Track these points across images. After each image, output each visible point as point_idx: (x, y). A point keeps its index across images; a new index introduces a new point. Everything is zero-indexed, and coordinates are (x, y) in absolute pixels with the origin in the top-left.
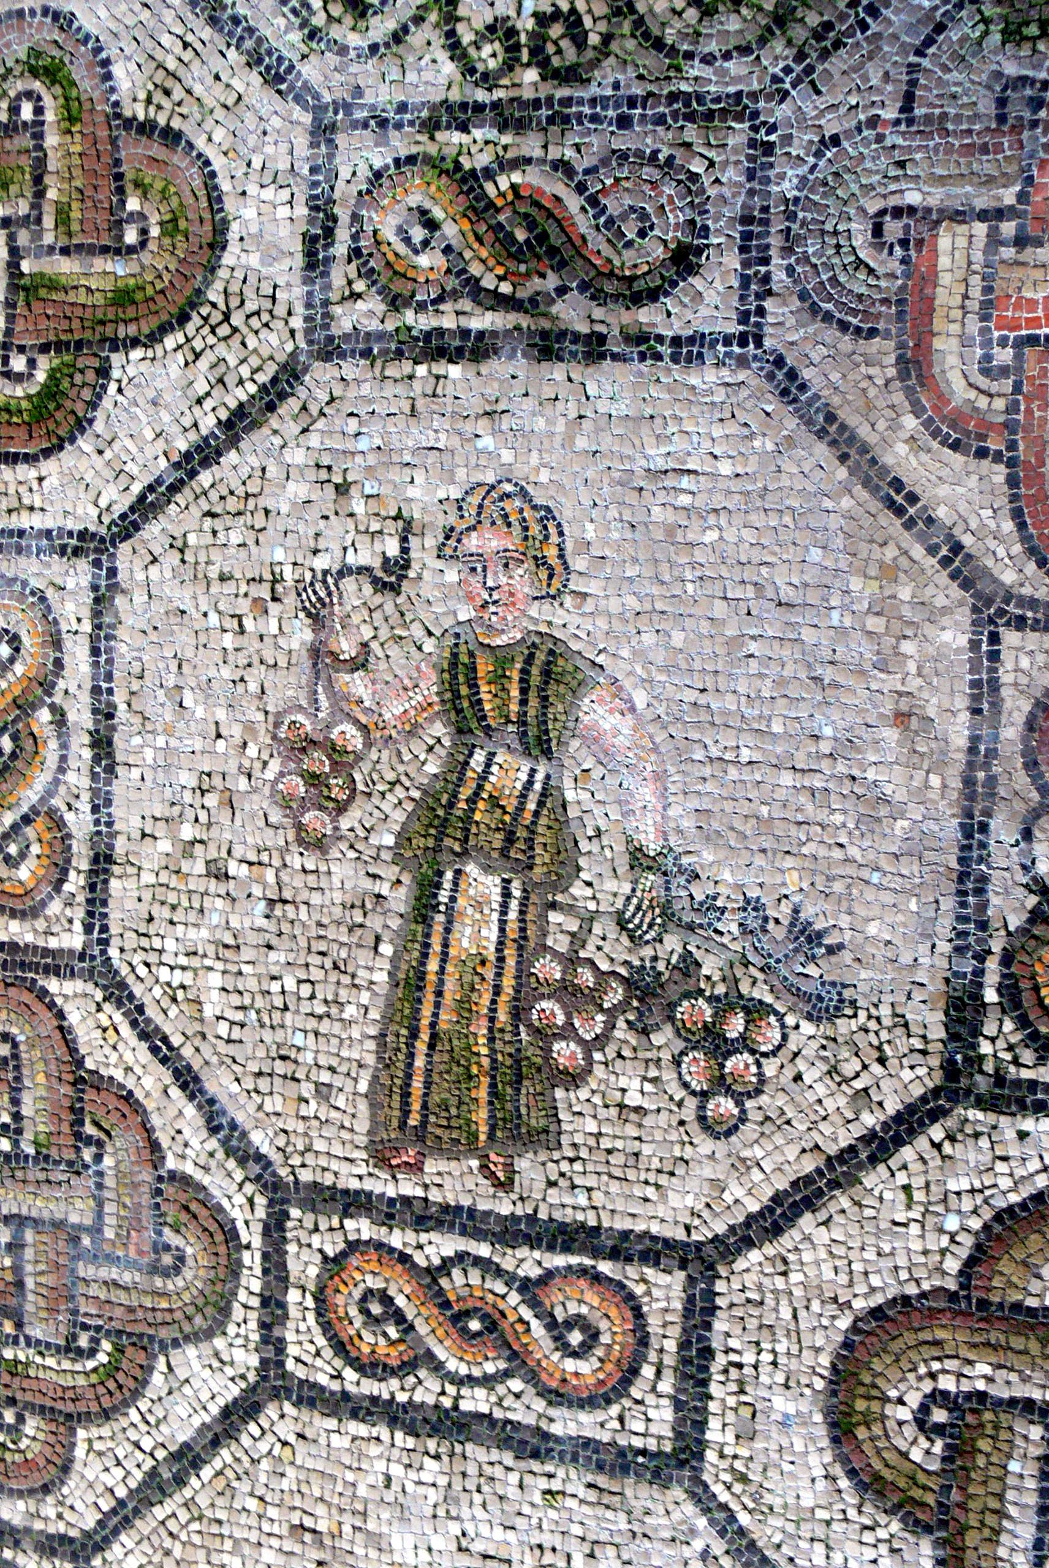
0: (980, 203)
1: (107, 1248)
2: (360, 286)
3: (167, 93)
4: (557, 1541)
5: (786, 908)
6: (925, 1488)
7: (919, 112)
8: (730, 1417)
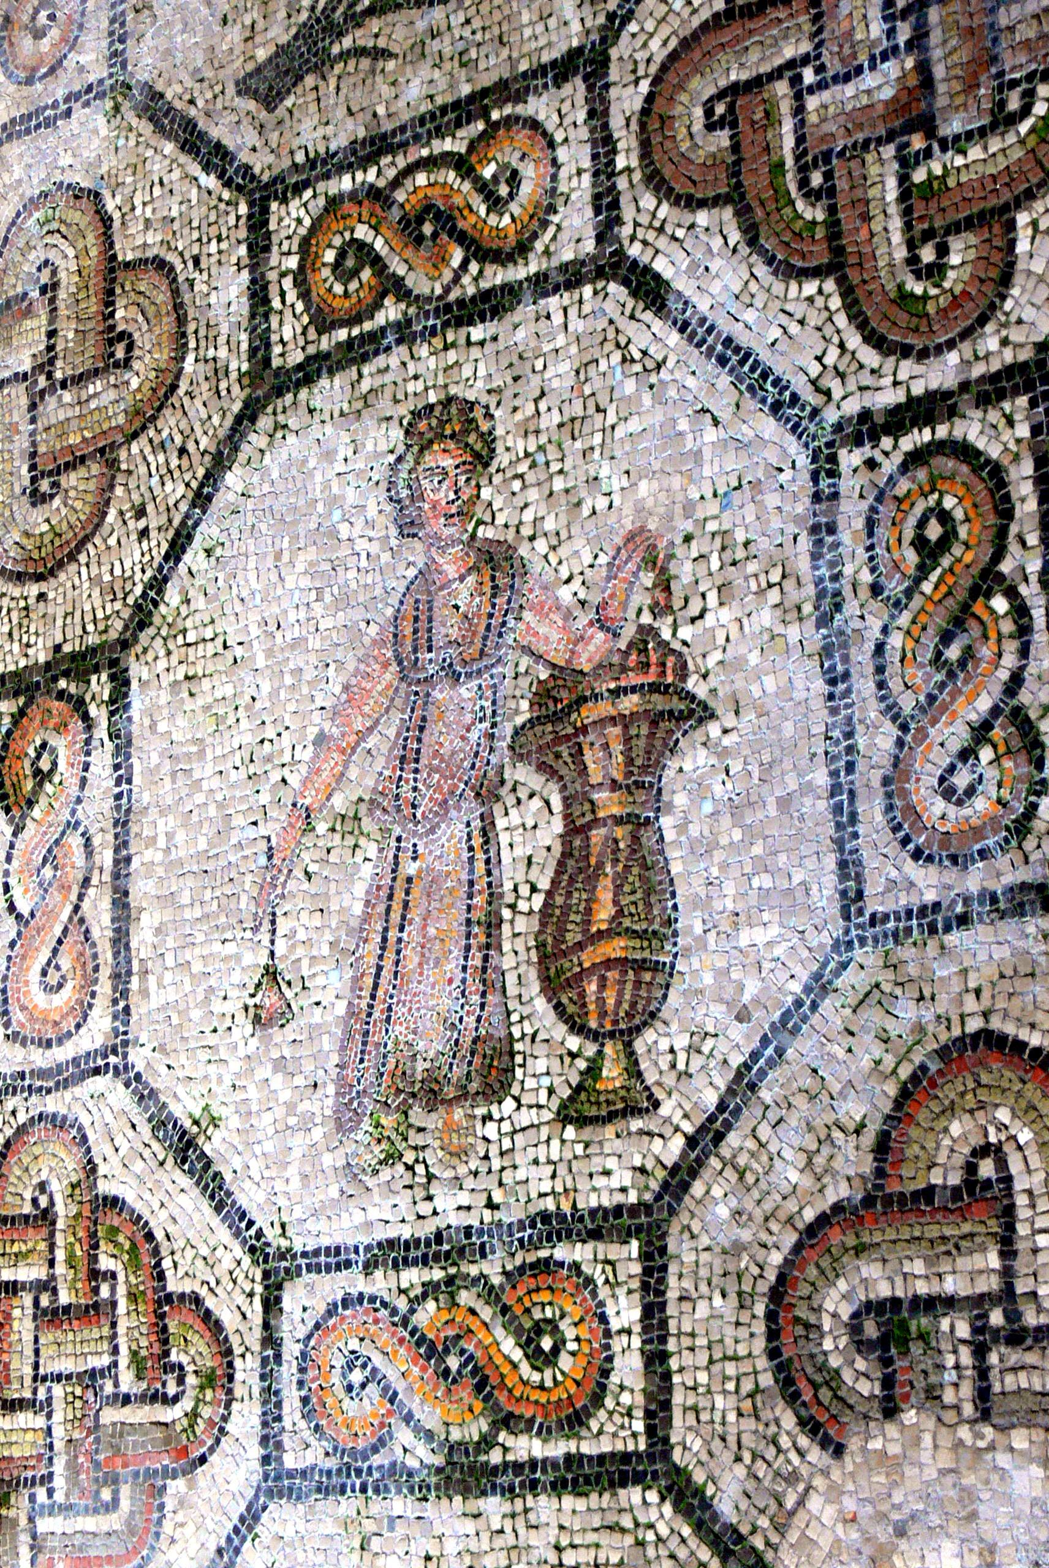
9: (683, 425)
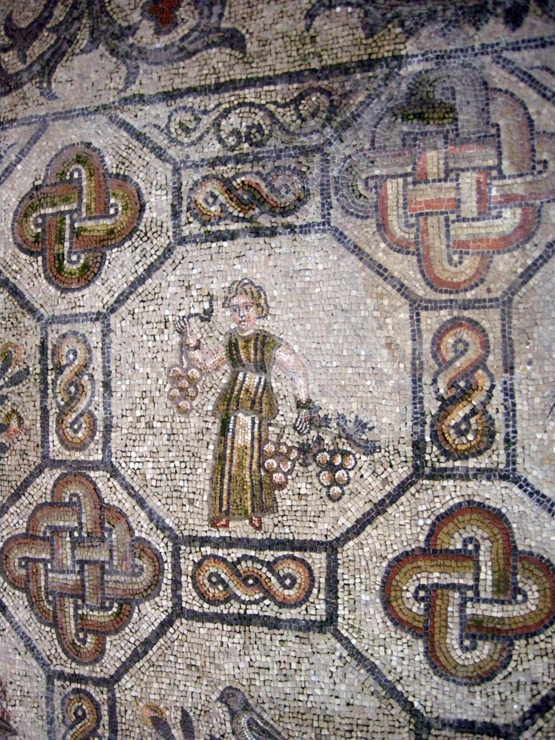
0: (400, 172)
1: (114, 568)
2: (191, 219)
3: (123, 164)
4: (286, 658)
5: (353, 416)
6: (419, 621)
7: (377, 145)
8: (346, 604)
9: (10, 650)
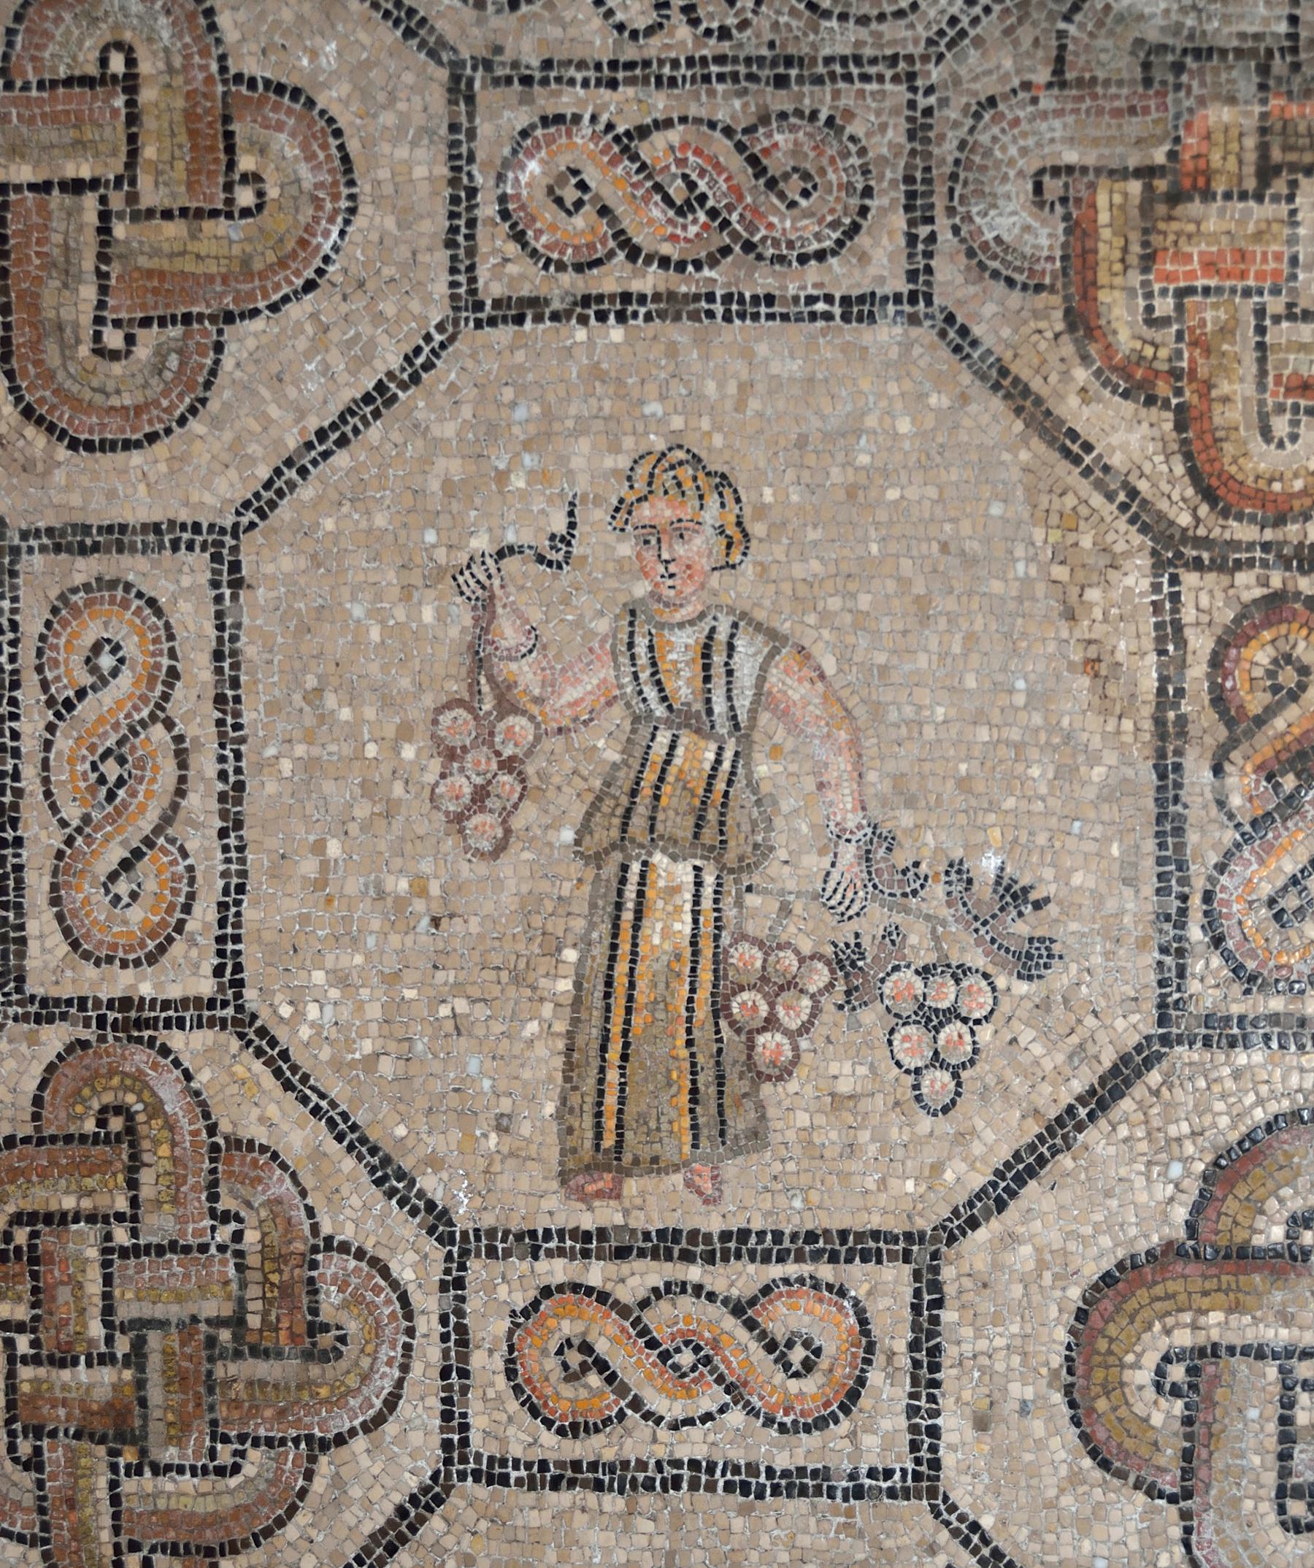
0: (1132, 163)
7: (1070, 76)
